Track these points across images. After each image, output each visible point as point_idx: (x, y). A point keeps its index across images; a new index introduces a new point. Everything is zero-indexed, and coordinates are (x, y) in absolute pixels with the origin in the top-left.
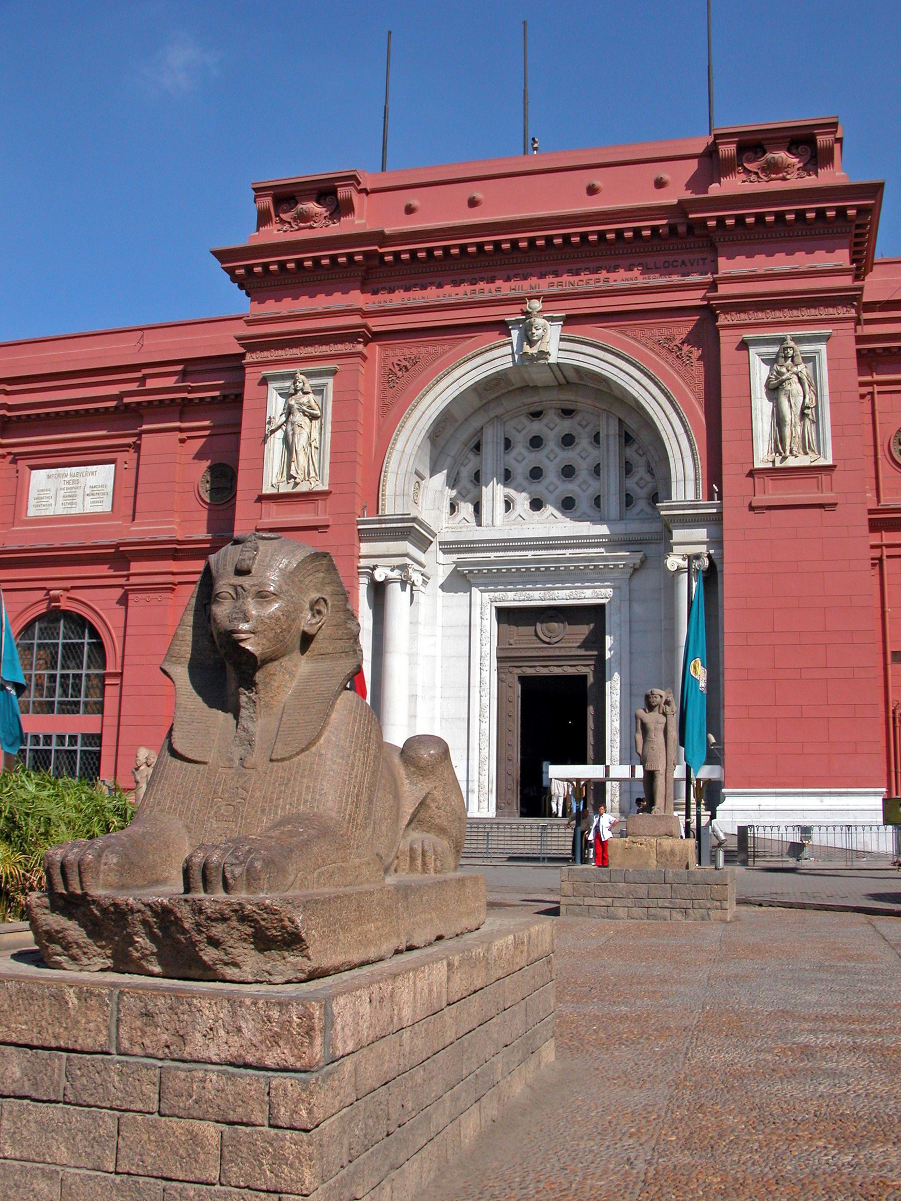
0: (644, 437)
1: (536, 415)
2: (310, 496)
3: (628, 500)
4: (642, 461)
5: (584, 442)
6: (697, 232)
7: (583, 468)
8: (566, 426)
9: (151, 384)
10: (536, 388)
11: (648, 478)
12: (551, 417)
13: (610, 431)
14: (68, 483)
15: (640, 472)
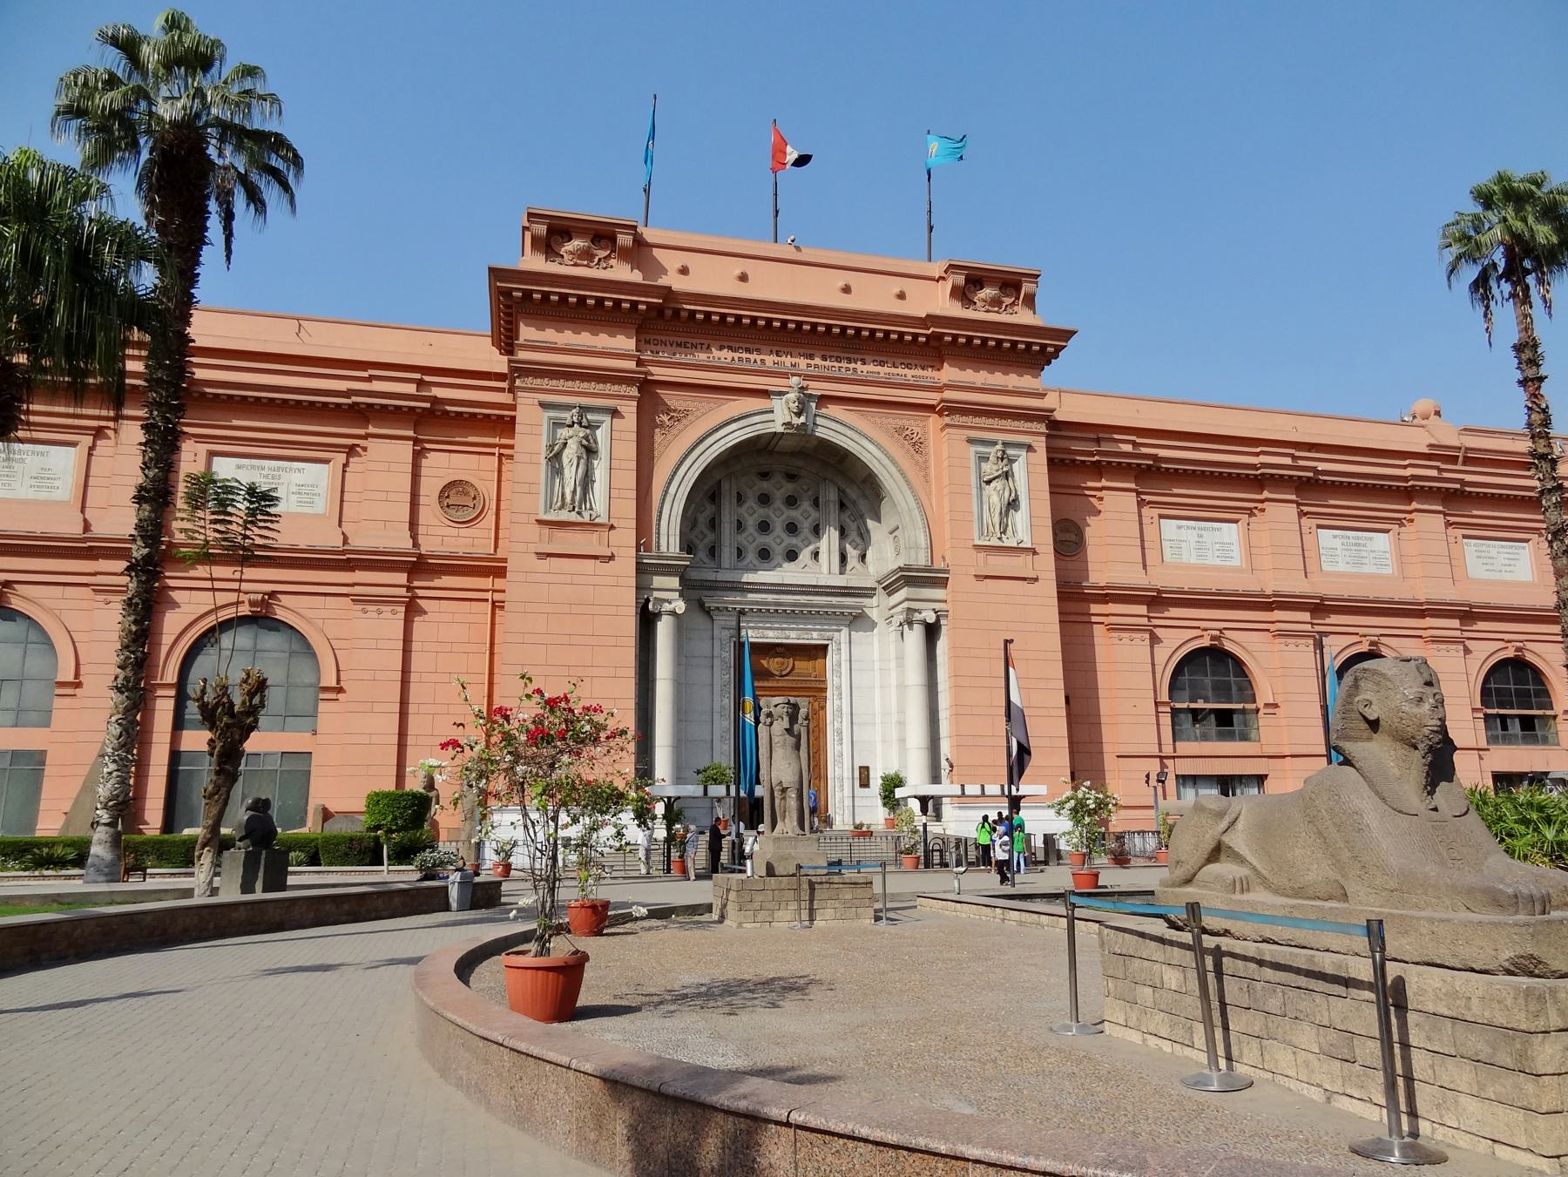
0: (863, 505)
1: (765, 475)
2: (592, 525)
3: (843, 558)
4: (853, 526)
5: (806, 505)
6: (933, 343)
7: (805, 527)
8: (789, 488)
9: (377, 386)
10: (771, 453)
11: (858, 540)
12: (778, 477)
13: (833, 495)
14: (266, 476)
15: (854, 535)
